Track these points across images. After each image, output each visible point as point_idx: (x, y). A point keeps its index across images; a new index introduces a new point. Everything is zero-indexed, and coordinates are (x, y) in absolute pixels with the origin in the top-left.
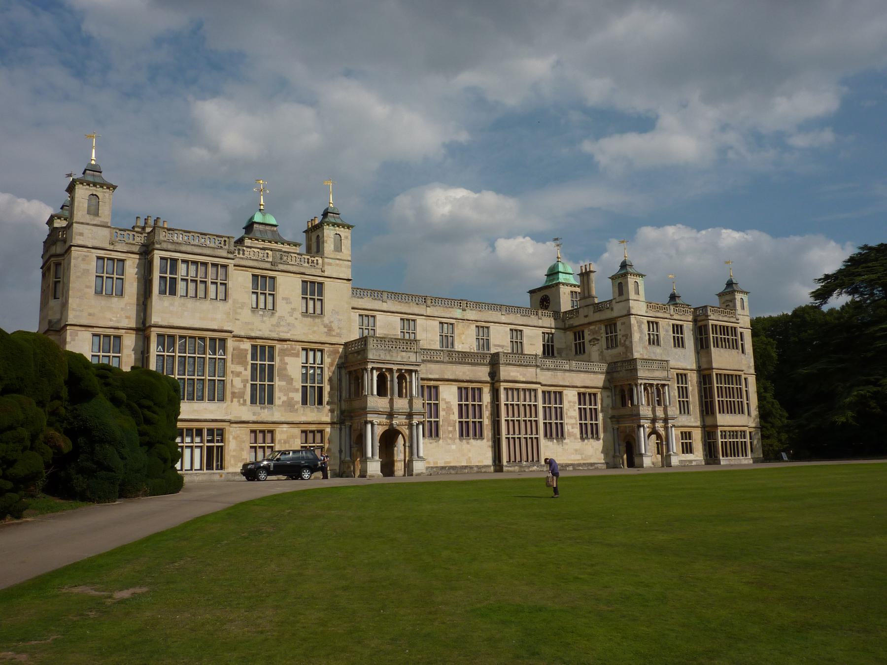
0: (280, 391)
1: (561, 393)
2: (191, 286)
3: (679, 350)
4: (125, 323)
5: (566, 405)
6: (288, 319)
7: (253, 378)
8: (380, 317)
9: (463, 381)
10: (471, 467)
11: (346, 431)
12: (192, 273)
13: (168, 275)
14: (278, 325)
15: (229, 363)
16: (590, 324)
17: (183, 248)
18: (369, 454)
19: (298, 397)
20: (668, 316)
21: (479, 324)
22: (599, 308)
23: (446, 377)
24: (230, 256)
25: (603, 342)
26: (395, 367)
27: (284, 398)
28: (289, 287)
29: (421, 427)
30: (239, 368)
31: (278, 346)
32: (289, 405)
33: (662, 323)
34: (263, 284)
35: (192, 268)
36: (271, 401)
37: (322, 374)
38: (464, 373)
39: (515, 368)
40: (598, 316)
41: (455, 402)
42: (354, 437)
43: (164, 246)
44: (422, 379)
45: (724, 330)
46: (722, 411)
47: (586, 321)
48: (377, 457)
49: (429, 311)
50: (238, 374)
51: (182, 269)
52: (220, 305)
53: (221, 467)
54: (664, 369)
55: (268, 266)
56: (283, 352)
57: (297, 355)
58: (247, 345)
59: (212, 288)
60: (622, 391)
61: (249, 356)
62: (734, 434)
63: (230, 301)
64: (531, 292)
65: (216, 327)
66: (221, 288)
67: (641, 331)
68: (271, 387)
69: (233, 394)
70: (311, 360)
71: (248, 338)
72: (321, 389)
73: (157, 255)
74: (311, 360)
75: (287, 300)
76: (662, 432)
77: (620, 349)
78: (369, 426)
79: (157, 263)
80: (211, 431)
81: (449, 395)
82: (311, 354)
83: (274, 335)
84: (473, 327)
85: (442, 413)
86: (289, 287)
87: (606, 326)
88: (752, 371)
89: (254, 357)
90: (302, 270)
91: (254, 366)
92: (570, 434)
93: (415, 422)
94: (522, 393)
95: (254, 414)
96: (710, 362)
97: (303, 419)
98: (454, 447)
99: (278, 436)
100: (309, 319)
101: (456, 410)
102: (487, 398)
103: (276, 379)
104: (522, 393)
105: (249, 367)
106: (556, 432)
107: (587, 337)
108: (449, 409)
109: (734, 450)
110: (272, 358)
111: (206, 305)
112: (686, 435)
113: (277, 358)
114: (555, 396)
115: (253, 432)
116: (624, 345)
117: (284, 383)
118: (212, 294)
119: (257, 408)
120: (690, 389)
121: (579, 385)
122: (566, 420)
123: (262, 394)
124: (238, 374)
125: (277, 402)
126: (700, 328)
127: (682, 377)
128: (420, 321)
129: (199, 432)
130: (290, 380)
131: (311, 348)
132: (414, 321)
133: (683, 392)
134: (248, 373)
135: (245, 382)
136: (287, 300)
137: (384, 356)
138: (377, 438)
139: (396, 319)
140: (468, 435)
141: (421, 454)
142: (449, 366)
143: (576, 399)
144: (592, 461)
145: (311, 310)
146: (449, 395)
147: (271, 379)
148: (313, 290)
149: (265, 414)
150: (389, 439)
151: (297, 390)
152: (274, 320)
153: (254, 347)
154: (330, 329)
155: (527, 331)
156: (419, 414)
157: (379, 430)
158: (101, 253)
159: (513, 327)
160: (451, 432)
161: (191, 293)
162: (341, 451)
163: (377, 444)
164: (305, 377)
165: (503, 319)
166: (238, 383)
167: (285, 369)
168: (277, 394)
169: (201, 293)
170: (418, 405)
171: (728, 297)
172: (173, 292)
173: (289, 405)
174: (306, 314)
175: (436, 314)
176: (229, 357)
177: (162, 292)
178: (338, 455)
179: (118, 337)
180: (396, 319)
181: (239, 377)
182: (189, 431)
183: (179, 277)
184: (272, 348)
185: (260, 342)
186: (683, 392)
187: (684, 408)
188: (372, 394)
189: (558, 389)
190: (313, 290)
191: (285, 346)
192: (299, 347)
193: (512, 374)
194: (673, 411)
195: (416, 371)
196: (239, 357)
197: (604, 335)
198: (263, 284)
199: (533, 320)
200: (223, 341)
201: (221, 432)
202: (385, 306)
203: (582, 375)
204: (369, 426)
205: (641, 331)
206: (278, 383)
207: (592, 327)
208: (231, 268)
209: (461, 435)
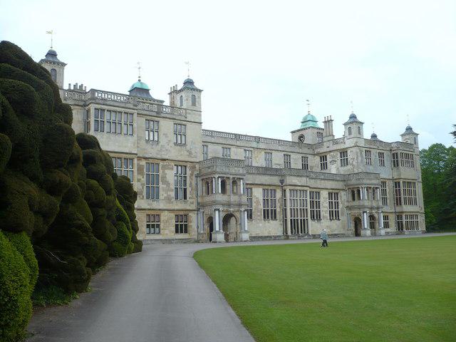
0: (163, 191)
1: (319, 193)
2: (113, 125)
5: (322, 200)
7: (148, 182)
8: (210, 146)
9: (265, 185)
10: (271, 237)
11: (200, 215)
12: (113, 118)
13: (99, 119)
14: (161, 150)
15: (136, 173)
16: (330, 151)
17: (108, 103)
18: (217, 229)
19: (173, 194)
20: (374, 147)
21: (266, 151)
22: (336, 142)
23: (256, 183)
24: (135, 108)
25: (339, 161)
26: (231, 177)
27: (166, 195)
29: (246, 212)
30: (140, 177)
32: (168, 199)
33: (373, 151)
35: (113, 114)
37: (185, 181)
38: (266, 180)
39: (295, 178)
40: (336, 147)
41: (261, 198)
42: (205, 219)
43: (97, 101)
44: (247, 184)
45: (407, 155)
46: (405, 203)
47: (328, 150)
48: (222, 231)
49: (238, 143)
51: (107, 115)
52: (130, 138)
54: (377, 178)
55: (155, 114)
59: (124, 127)
60: (353, 192)
61: (145, 170)
62: (412, 217)
63: (135, 135)
64: (293, 132)
65: (128, 152)
66: (130, 127)
67: (362, 157)
70: (180, 172)
71: (144, 158)
72: (185, 190)
73: (92, 107)
74: (180, 172)
76: (376, 215)
77: (349, 167)
78: (217, 212)
79: (92, 112)
82: (180, 168)
83: (159, 157)
84: (263, 153)
85: (254, 204)
87: (341, 153)
88: (420, 180)
90: (174, 117)
92: (324, 217)
93: (243, 209)
94: (299, 192)
95: (149, 204)
96: (400, 175)
97: (176, 208)
98: (261, 224)
99: (162, 218)
101: (262, 203)
102: (279, 194)
103: (161, 183)
104: (299, 192)
105: (145, 176)
106: (317, 216)
107: (329, 159)
108: (258, 202)
109: (412, 226)
111: (122, 138)
112: (386, 218)
113: (161, 171)
114: (315, 194)
115: (148, 215)
116: (352, 164)
117: (165, 186)
118: (124, 131)
119: (150, 201)
120: (388, 191)
121: (329, 188)
122: (322, 209)
124: (139, 180)
125: (161, 197)
126: (394, 154)
127: (384, 183)
130: (168, 184)
131: (182, 165)
132: (229, 149)
133: (384, 192)
135: (143, 185)
138: (222, 219)
139: (219, 148)
140: (268, 217)
141: (246, 229)
142: (258, 176)
143: (327, 196)
144: (336, 233)
145: (179, 142)
149: (155, 205)
150: (227, 219)
151: (172, 191)
152: (159, 147)
154: (190, 153)
155: (293, 156)
156: (245, 205)
157: (223, 215)
159: (285, 153)
160: (258, 216)
161: (113, 130)
162: (198, 227)
163: (222, 223)
165: (280, 148)
167: (165, 177)
168: (161, 192)
169: (118, 131)
170: (244, 199)
171: (407, 137)
173: (168, 199)
175: (242, 144)
178: (196, 229)
183: (105, 120)
186: (384, 192)
187: (384, 200)
188: (218, 193)
189: (318, 190)
191: (165, 163)
192: (173, 164)
193: (293, 181)
194: (381, 204)
195: (242, 179)
197: (339, 158)
199: (298, 150)
202: (213, 140)
203: (331, 182)
204: (217, 212)
205: (362, 157)
206: (161, 185)
207: (332, 154)
208: (135, 115)
209: (264, 217)
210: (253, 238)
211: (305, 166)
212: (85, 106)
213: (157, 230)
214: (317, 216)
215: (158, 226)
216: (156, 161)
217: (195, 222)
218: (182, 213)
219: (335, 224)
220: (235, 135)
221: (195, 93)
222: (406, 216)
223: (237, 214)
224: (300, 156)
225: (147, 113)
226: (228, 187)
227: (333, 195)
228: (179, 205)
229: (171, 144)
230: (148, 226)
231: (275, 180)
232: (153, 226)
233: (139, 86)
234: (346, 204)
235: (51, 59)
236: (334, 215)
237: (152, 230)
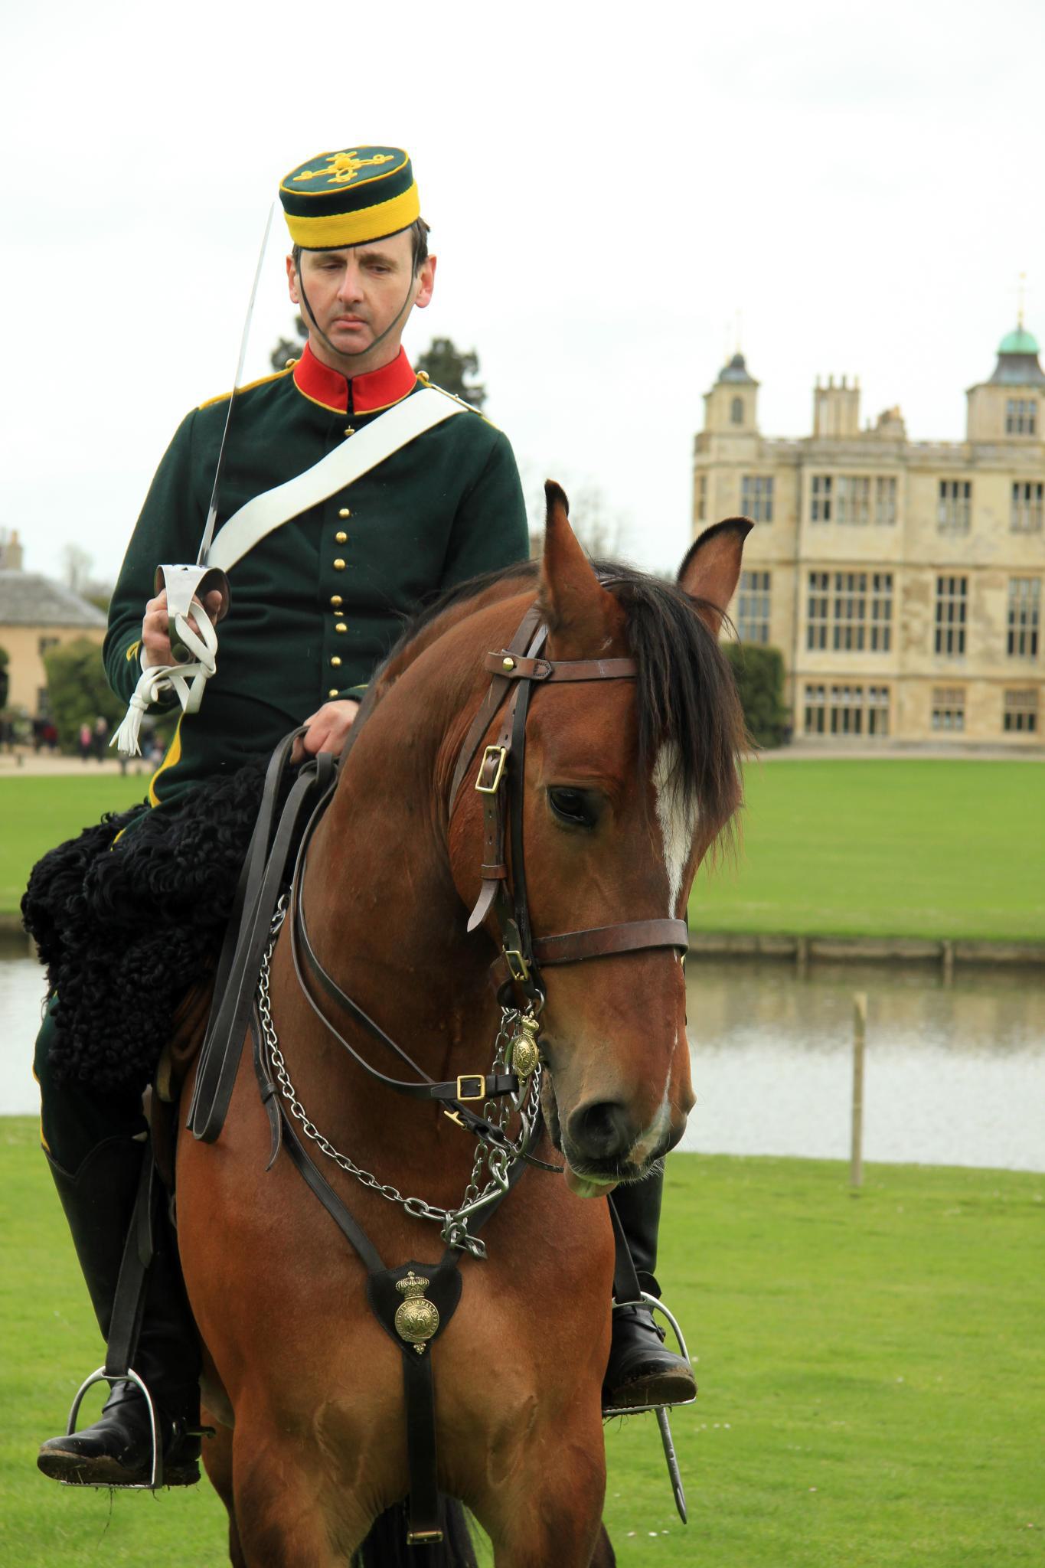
4: (775, 554)
7: (939, 618)
19: (1001, 644)
30: (916, 606)
31: (973, 578)
32: (988, 656)
34: (955, 490)
36: (962, 649)
50: (916, 615)
51: (839, 489)
53: (886, 732)
56: (981, 584)
57: (999, 586)
58: (930, 578)
68: (962, 634)
69: (909, 643)
73: (809, 472)
75: (988, 511)
80: (873, 690)
83: (969, 560)
89: (940, 591)
91: (940, 606)
100: (1020, 538)
110: (964, 591)
119: (943, 658)
123: (951, 642)
124: (916, 615)
129: (859, 690)
130: (988, 621)
134: (930, 613)
135: (926, 625)
136: (988, 511)
147: (963, 618)
151: (997, 635)
153: (940, 582)
158: (747, 471)
164: (1012, 618)
166: (916, 626)
172: (827, 515)
173: (988, 656)
174: (1015, 529)
176: (897, 596)
177: (815, 517)
179: (767, 577)
181: (917, 617)
182: (847, 690)
184: (964, 582)
185: (947, 573)
191: (985, 574)
192: (1004, 577)
198: (955, 490)
200: (889, 580)
201: (885, 691)
206: (972, 625)
212: (798, 466)
213: (957, 722)
215: (960, 714)
216: (958, 574)
218: (1022, 687)
225: (944, 465)
229: (1004, 530)
230: (936, 713)
232: (948, 713)
233: (1011, 347)
235: (734, 376)
237: (946, 721)
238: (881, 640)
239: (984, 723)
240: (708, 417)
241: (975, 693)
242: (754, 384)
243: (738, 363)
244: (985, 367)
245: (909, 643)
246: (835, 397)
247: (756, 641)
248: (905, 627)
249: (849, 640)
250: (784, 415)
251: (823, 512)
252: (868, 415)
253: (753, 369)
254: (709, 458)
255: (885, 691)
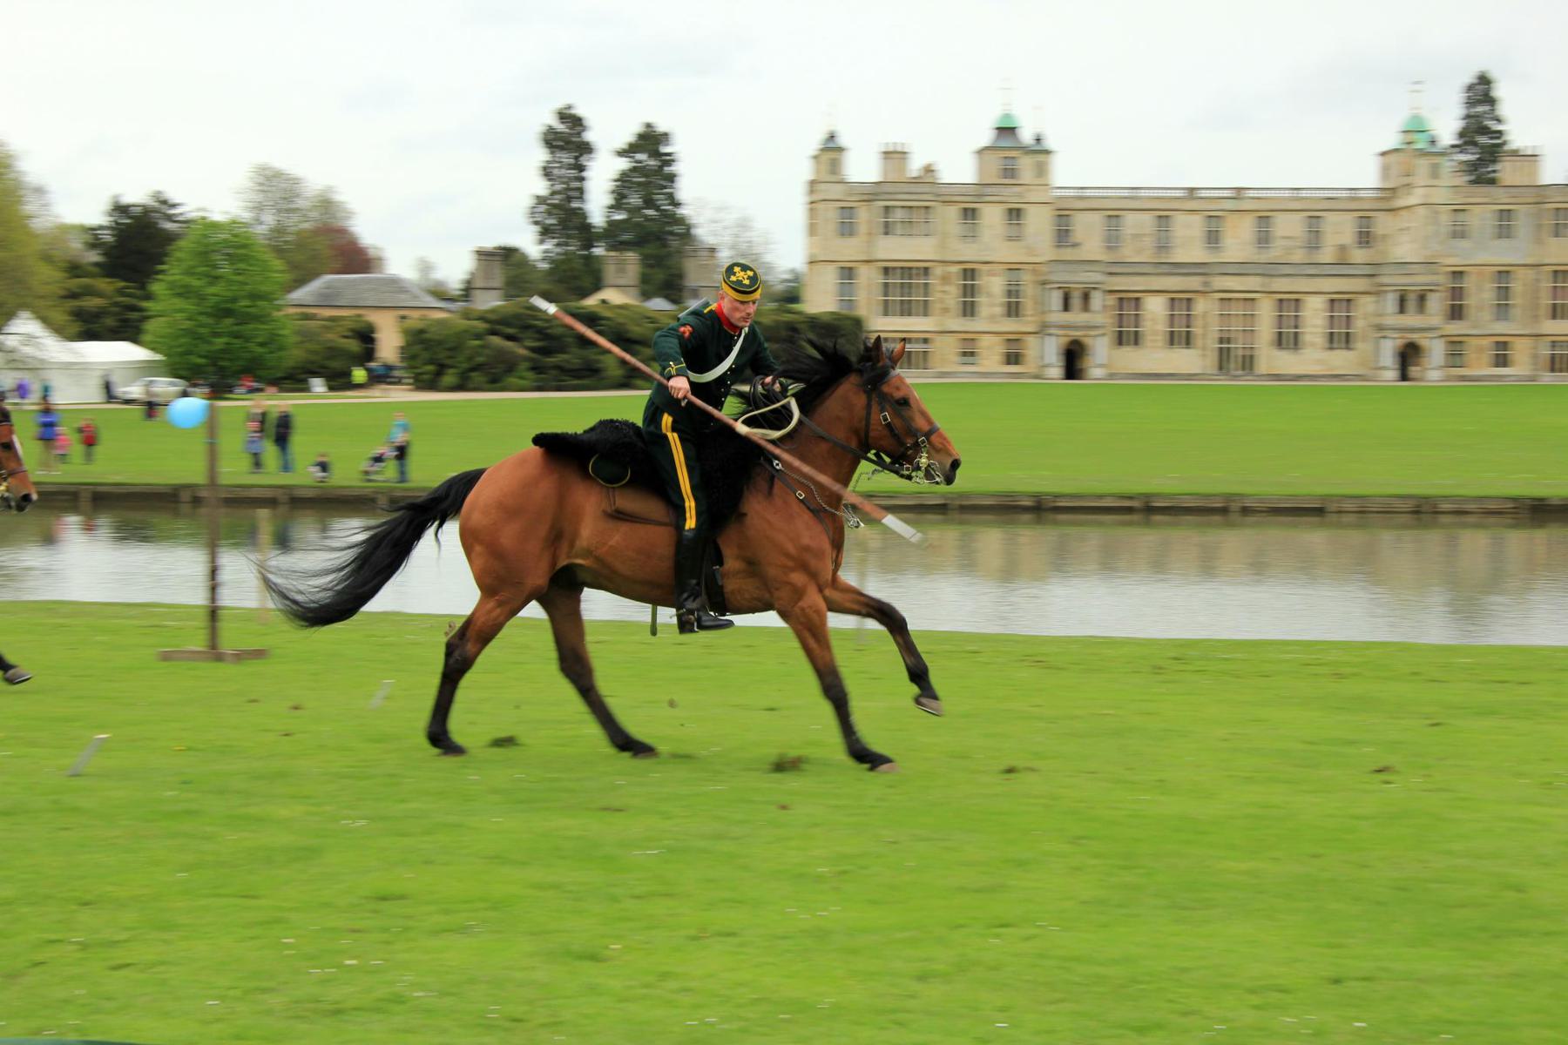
3: (1504, 243)
6: (992, 242)
8: (1130, 218)
19: (999, 310)
28: (992, 216)
30: (947, 288)
34: (969, 214)
51: (899, 215)
58: (955, 269)
81: (1155, 308)
86: (992, 216)
92: (1313, 345)
123: (969, 310)
128: (1180, 219)
131: (1013, 268)
133: (1504, 292)
137: (1067, 277)
143: (1327, 306)
146: (1155, 308)
148: (1015, 214)
173: (992, 318)
180: (1147, 218)
181: (947, 294)
186: (1504, 292)
190: (1015, 214)
196: (945, 279)
198: (969, 214)
210: (1112, 376)
211: (1365, 238)
214: (1288, 339)
217: (1032, 347)
219: (1341, 361)
220: (1192, 190)
221: (1041, 158)
222: (1554, 344)
223: (1087, 341)
224: (1349, 216)
226: (1076, 301)
227: (1340, 304)
228: (1011, 325)
231: (1194, 283)
234: (1377, 321)
236: (1340, 338)
238: (925, 310)
239: (991, 359)
240: (818, 171)
241: (986, 341)
242: (840, 149)
243: (832, 137)
244: (986, 137)
245: (946, 310)
246: (895, 157)
247: (844, 312)
248: (942, 301)
249: (906, 310)
250: (863, 168)
251: (887, 230)
252: (915, 166)
253: (843, 140)
254: (815, 198)
255: (926, 341)
